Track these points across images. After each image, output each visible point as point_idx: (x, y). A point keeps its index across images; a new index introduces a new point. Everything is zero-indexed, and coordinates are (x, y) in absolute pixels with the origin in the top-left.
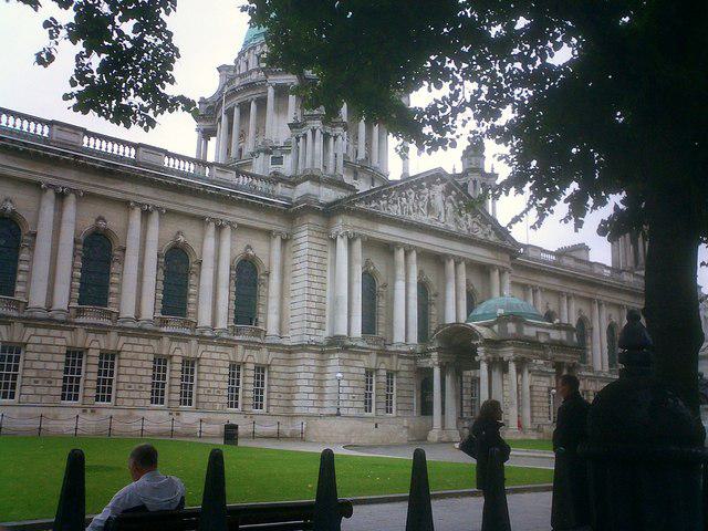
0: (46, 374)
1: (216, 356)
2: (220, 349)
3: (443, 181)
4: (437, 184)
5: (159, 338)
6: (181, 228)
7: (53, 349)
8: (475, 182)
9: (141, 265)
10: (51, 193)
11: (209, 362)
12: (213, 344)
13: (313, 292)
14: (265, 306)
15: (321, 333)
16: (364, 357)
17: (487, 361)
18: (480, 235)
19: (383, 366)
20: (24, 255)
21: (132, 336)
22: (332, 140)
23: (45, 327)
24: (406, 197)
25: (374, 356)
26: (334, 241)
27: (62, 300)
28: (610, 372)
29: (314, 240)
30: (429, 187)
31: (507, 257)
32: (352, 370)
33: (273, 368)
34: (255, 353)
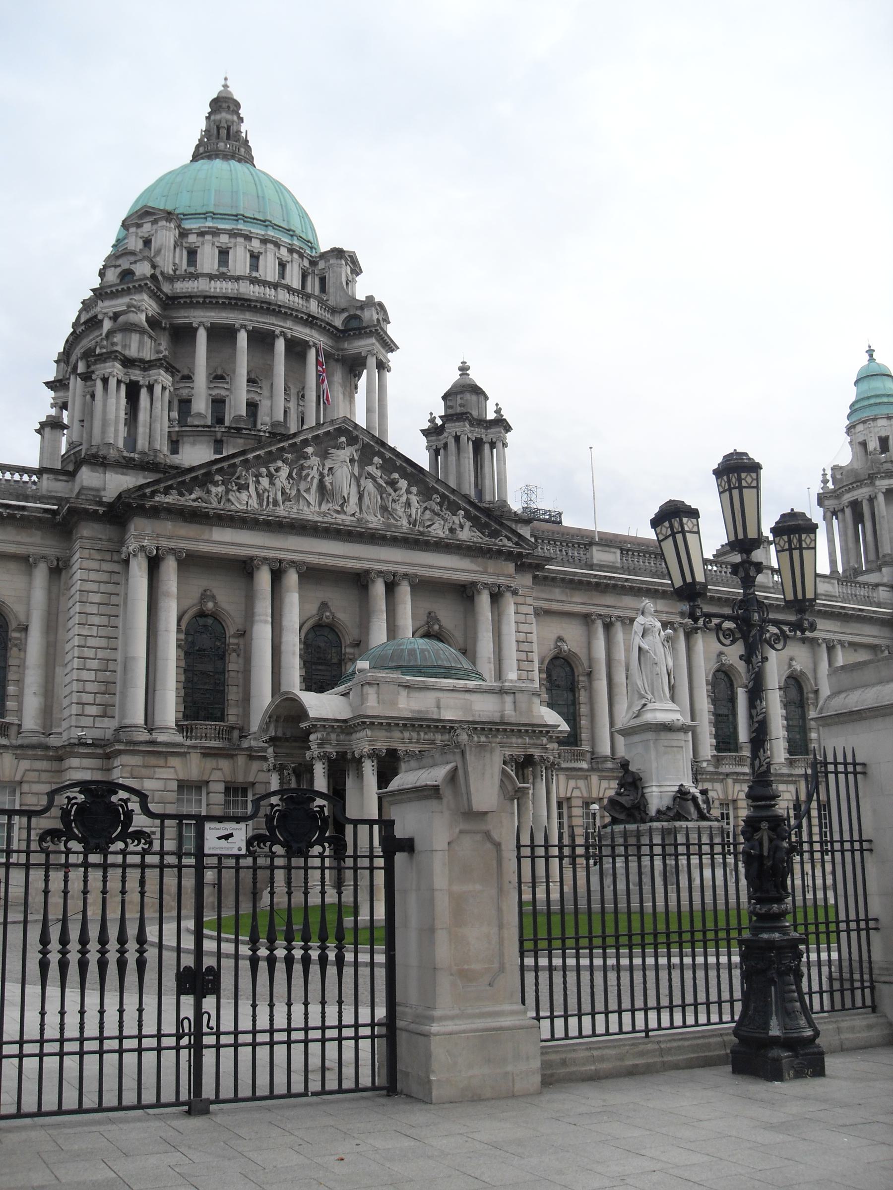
3: (352, 440)
4: (339, 447)
8: (457, 439)
14: (20, 682)
15: (106, 723)
16: (174, 761)
17: (325, 757)
18: (439, 530)
19: (217, 775)
22: (144, 393)
24: (270, 476)
25: (195, 758)
26: (126, 562)
28: (791, 763)
29: (94, 565)
30: (324, 455)
31: (510, 567)
33: (25, 788)
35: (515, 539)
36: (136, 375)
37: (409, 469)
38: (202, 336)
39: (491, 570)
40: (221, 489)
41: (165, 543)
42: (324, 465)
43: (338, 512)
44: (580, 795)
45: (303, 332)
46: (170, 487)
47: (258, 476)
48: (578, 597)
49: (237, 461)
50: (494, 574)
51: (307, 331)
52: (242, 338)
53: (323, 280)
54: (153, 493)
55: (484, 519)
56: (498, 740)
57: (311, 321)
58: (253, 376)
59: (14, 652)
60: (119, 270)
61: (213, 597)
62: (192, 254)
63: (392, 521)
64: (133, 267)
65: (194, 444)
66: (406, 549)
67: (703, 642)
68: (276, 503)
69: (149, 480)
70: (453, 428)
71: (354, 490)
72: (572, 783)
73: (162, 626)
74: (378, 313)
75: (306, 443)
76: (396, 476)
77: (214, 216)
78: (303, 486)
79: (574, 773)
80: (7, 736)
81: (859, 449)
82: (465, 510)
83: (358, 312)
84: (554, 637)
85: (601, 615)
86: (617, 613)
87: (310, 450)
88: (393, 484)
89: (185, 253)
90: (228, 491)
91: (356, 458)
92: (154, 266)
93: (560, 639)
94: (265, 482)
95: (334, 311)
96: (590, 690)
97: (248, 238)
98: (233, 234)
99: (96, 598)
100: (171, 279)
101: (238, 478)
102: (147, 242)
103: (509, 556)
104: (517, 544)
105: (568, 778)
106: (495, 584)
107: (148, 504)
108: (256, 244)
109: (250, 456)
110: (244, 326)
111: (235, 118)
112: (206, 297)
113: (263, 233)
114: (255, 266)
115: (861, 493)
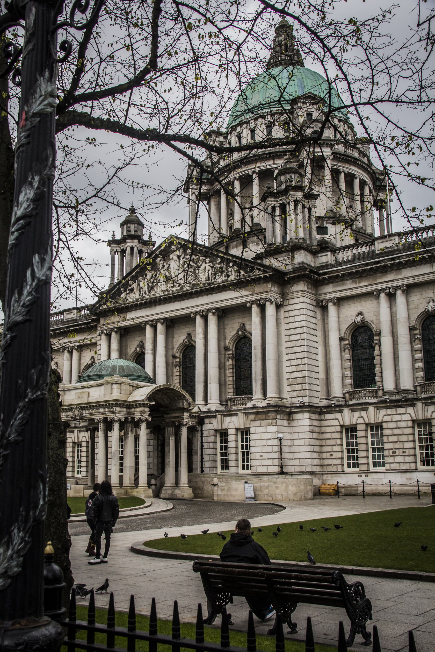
35: (262, 269)
37: (204, 250)
40: (123, 295)
41: (110, 326)
43: (172, 287)
44: (363, 422)
49: (129, 278)
50: (258, 294)
51: (272, 162)
54: (100, 306)
56: (93, 411)
66: (210, 294)
72: (357, 414)
74: (313, 128)
79: (355, 407)
85: (381, 290)
87: (158, 260)
90: (127, 294)
91: (179, 254)
93: (360, 314)
98: (240, 124)
101: (130, 286)
104: (264, 272)
106: (256, 300)
109: (134, 273)
110: (235, 179)
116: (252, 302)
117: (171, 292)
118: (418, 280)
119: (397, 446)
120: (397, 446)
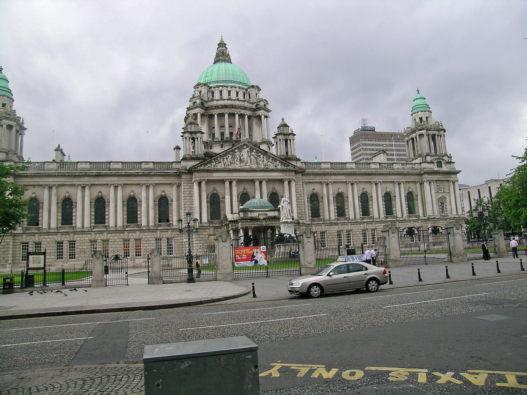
0: (83, 250)
1: (149, 237)
2: (150, 234)
5: (124, 233)
6: (132, 189)
7: (85, 241)
8: (280, 140)
9: (116, 206)
10: (80, 187)
11: (145, 239)
12: (147, 232)
13: (187, 206)
14: (172, 214)
16: (207, 230)
17: (232, 229)
18: (272, 167)
20: (74, 210)
21: (113, 233)
22: (196, 139)
23: (81, 234)
24: (227, 158)
25: (212, 229)
27: (87, 224)
29: (186, 185)
30: (241, 151)
32: (201, 236)
34: (166, 233)
36: (194, 136)
37: (263, 152)
38: (216, 116)
39: (288, 175)
40: (214, 163)
41: (202, 178)
42: (241, 154)
43: (245, 165)
45: (243, 112)
46: (202, 165)
47: (224, 159)
48: (318, 178)
49: (218, 156)
51: (244, 111)
52: (226, 116)
53: (249, 94)
54: (198, 167)
55: (284, 162)
57: (245, 108)
58: (231, 125)
59: (170, 207)
60: (193, 102)
61: (216, 189)
62: (213, 93)
63: (260, 166)
64: (196, 101)
65: (216, 146)
67: (357, 186)
68: (228, 165)
69: (198, 163)
70: (279, 137)
71: (249, 159)
72: (317, 227)
73: (202, 198)
75: (236, 149)
76: (260, 154)
77: (218, 82)
78: (236, 160)
80: (170, 227)
81: (414, 121)
82: (279, 160)
83: (259, 103)
84: (312, 189)
86: (330, 181)
87: (236, 151)
88: (259, 156)
89: (211, 93)
90: (216, 164)
92: (202, 100)
93: (314, 189)
94: (225, 160)
95: (252, 103)
96: (322, 202)
97: (227, 87)
99: (187, 193)
100: (206, 102)
102: (200, 92)
103: (292, 171)
104: (294, 168)
105: (316, 226)
107: (196, 170)
108: (229, 88)
109: (221, 154)
110: (227, 113)
111: (225, 48)
112: (216, 106)
113: (231, 85)
114: (229, 95)
115: (413, 136)
116: (286, 179)
117: (245, 168)
118: (337, 181)
119: (332, 239)
120: (332, 239)
